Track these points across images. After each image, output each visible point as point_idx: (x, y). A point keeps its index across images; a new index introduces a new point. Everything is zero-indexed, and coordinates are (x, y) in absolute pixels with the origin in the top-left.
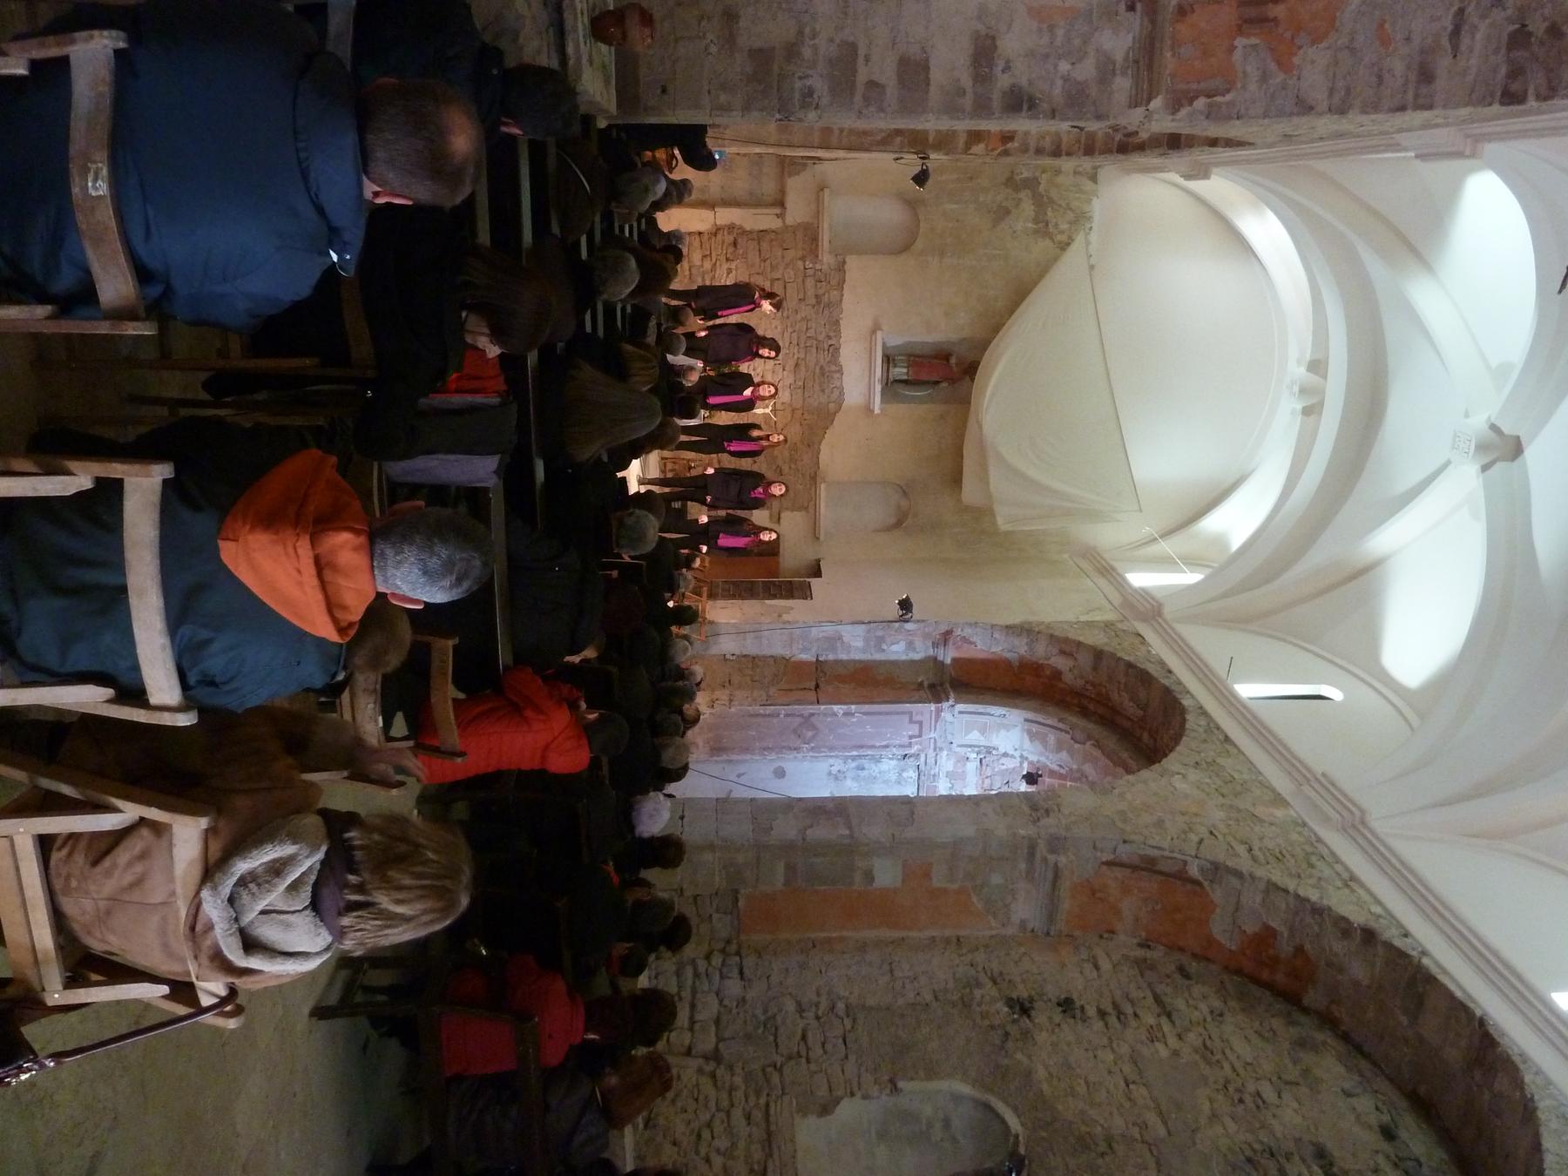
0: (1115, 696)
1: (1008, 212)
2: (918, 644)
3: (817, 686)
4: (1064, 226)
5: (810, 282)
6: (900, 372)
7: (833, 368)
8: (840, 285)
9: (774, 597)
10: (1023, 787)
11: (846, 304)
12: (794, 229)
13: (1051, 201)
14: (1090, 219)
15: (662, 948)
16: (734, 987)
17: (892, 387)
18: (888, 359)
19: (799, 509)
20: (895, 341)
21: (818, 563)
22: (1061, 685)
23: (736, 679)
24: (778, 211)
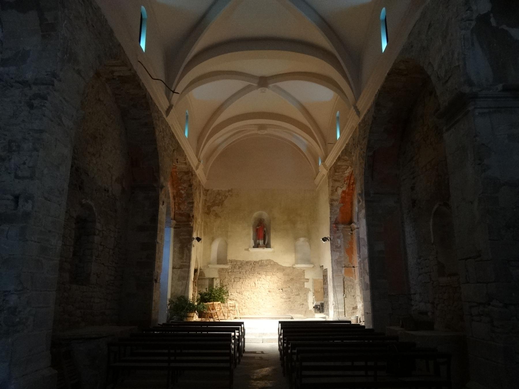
0: (347, 175)
1: (216, 213)
2: (338, 235)
3: (354, 267)
4: (220, 197)
5: (235, 270)
6: (261, 242)
7: (260, 263)
8: (236, 261)
9: (327, 281)
10: (203, 238)
11: (242, 260)
12: (220, 275)
13: (214, 202)
14: (218, 191)
15: (162, 315)
16: (417, 297)
17: (267, 245)
18: (257, 246)
19: (304, 273)
20: (252, 243)
21: (321, 267)
22: (347, 190)
23: (353, 294)
24: (215, 280)
